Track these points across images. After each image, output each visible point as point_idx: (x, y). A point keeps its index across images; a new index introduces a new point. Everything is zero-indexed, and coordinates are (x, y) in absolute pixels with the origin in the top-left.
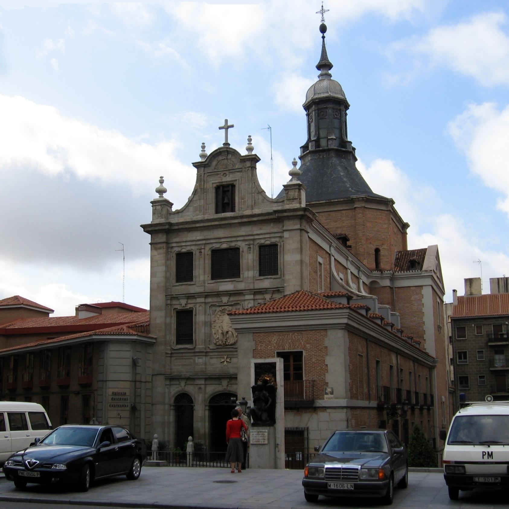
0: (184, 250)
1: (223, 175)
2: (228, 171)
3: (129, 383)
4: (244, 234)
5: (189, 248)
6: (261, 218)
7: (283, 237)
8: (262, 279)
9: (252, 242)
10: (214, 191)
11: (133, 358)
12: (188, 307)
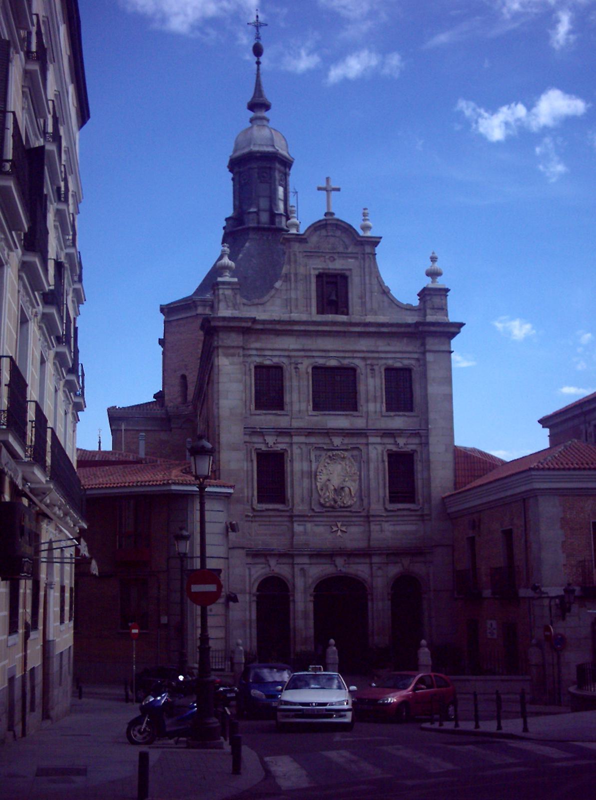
0: (267, 362)
1: (329, 259)
2: (337, 255)
3: (222, 560)
4: (364, 349)
5: (276, 360)
6: (394, 329)
7: (425, 359)
8: (391, 416)
9: (375, 362)
10: (314, 280)
11: (226, 523)
12: (279, 449)
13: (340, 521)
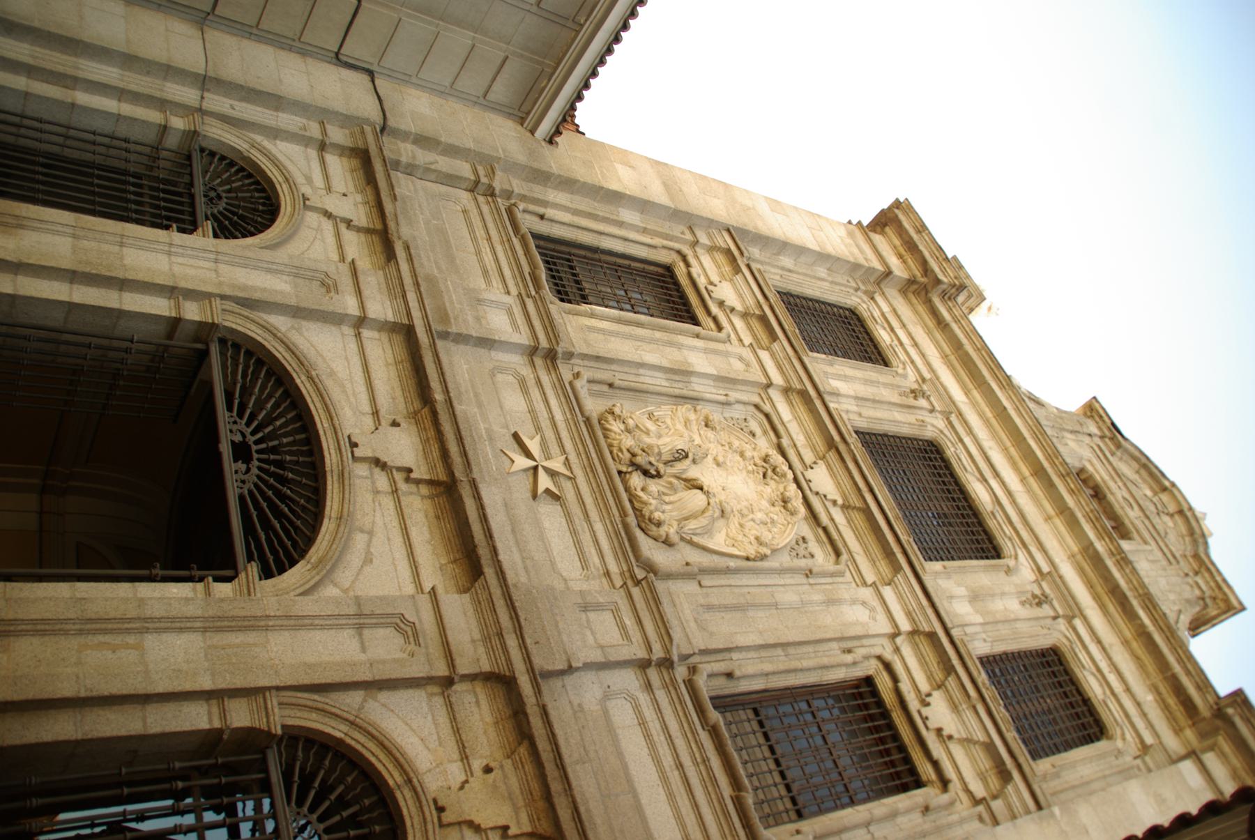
13: (570, 469)
